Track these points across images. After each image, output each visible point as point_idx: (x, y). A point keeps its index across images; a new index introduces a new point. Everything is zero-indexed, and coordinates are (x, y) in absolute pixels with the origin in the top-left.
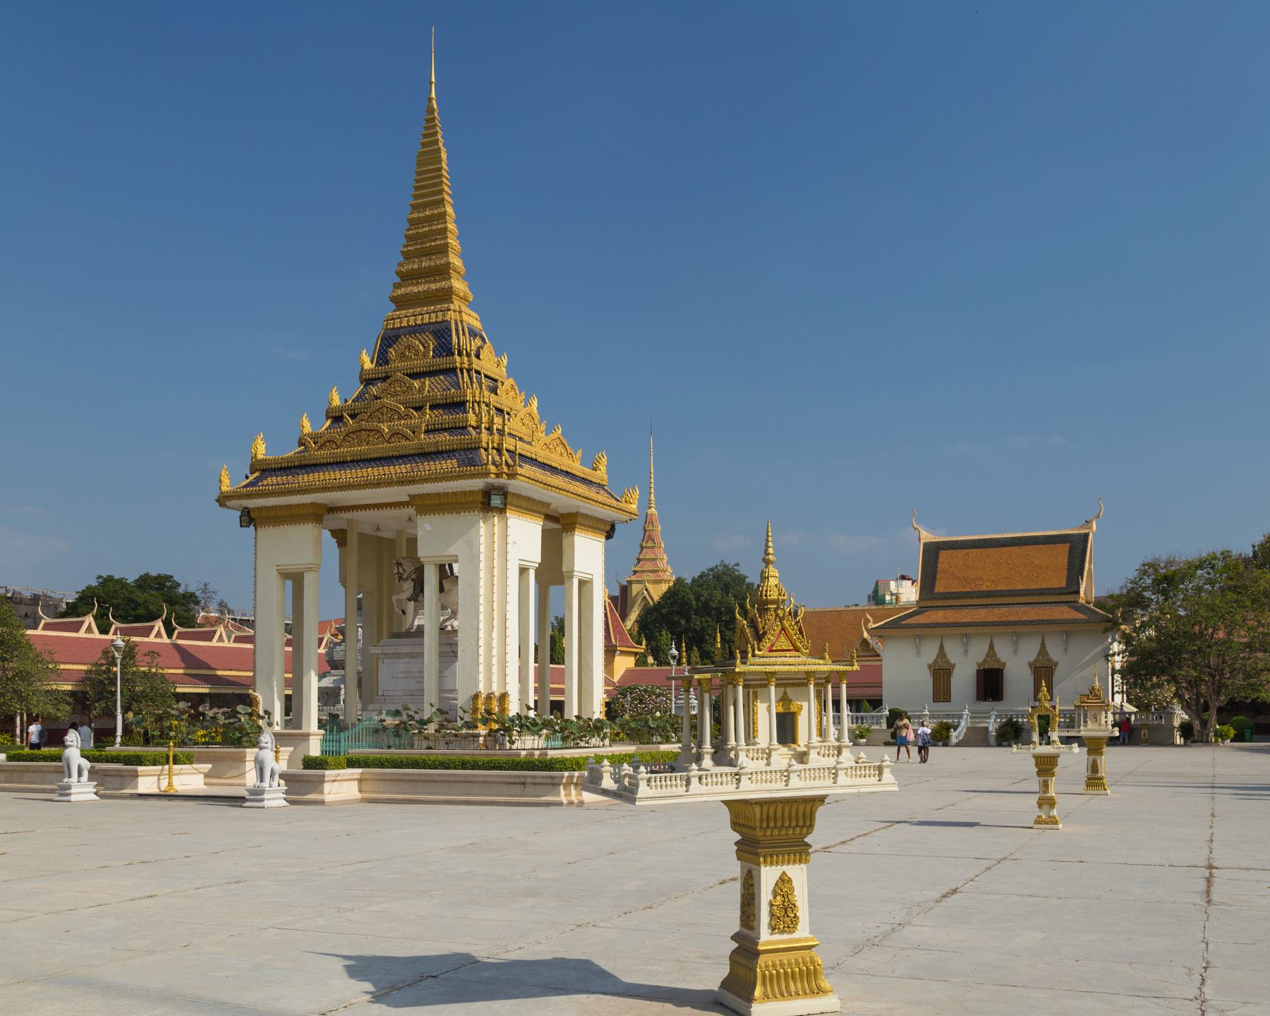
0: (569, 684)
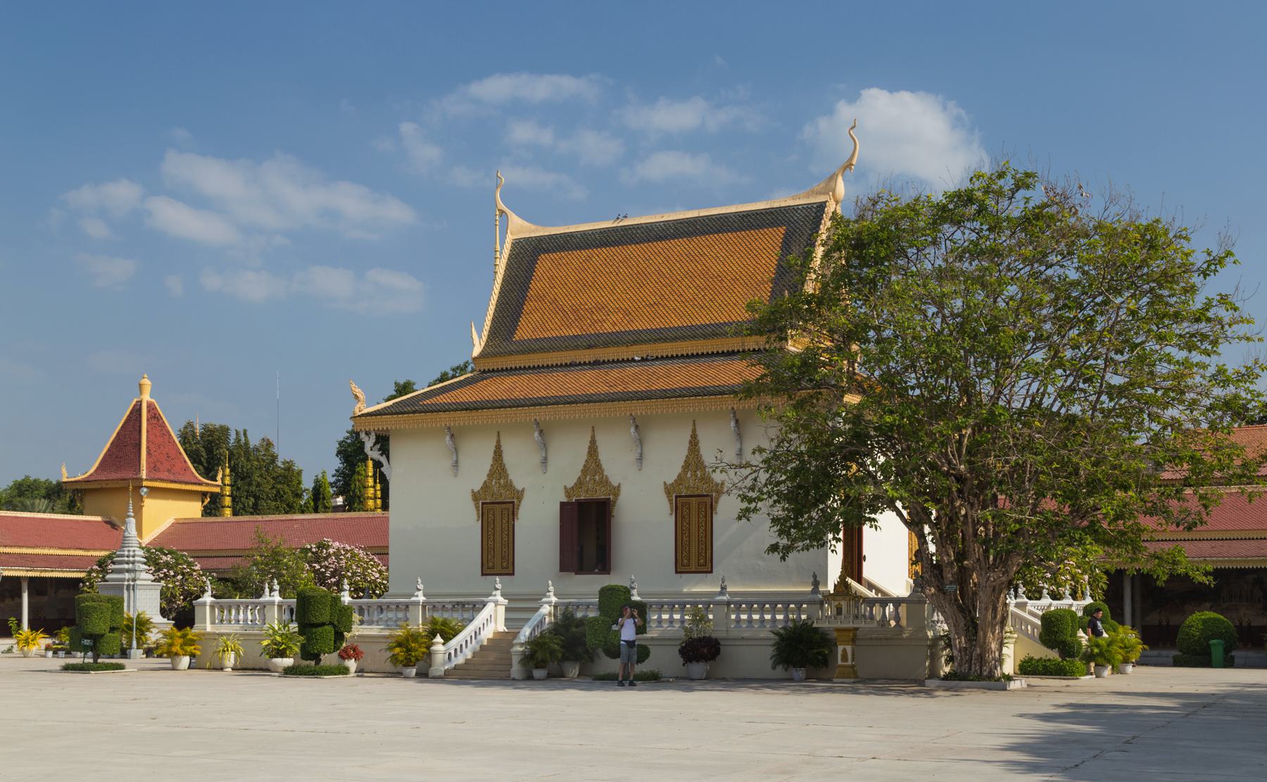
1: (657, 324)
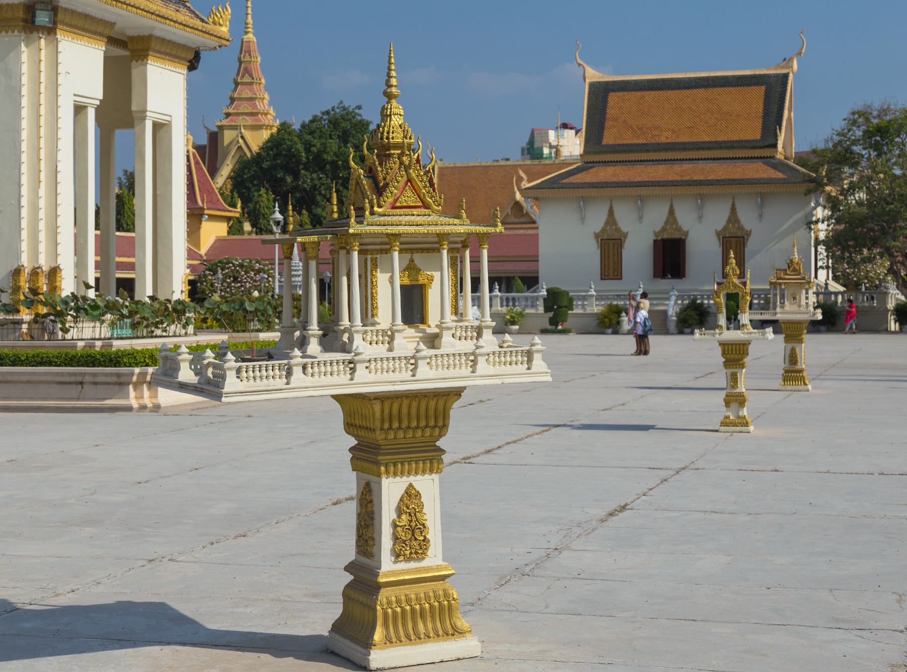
0: (141, 256)
1: (694, 139)
